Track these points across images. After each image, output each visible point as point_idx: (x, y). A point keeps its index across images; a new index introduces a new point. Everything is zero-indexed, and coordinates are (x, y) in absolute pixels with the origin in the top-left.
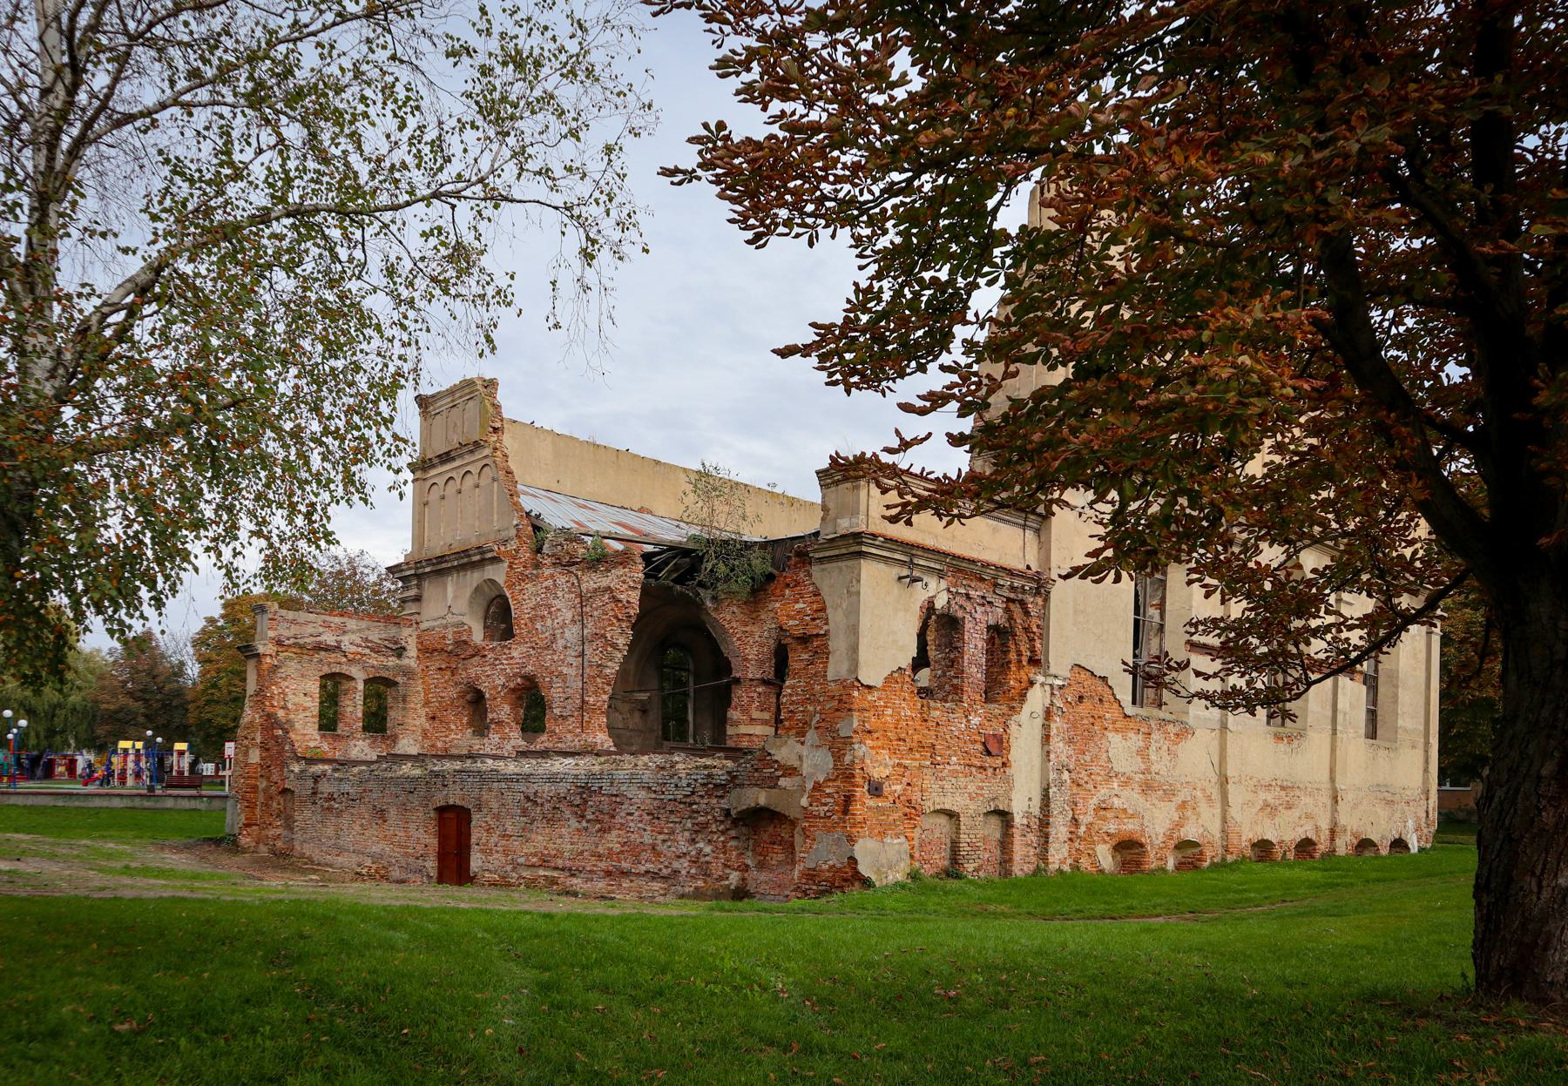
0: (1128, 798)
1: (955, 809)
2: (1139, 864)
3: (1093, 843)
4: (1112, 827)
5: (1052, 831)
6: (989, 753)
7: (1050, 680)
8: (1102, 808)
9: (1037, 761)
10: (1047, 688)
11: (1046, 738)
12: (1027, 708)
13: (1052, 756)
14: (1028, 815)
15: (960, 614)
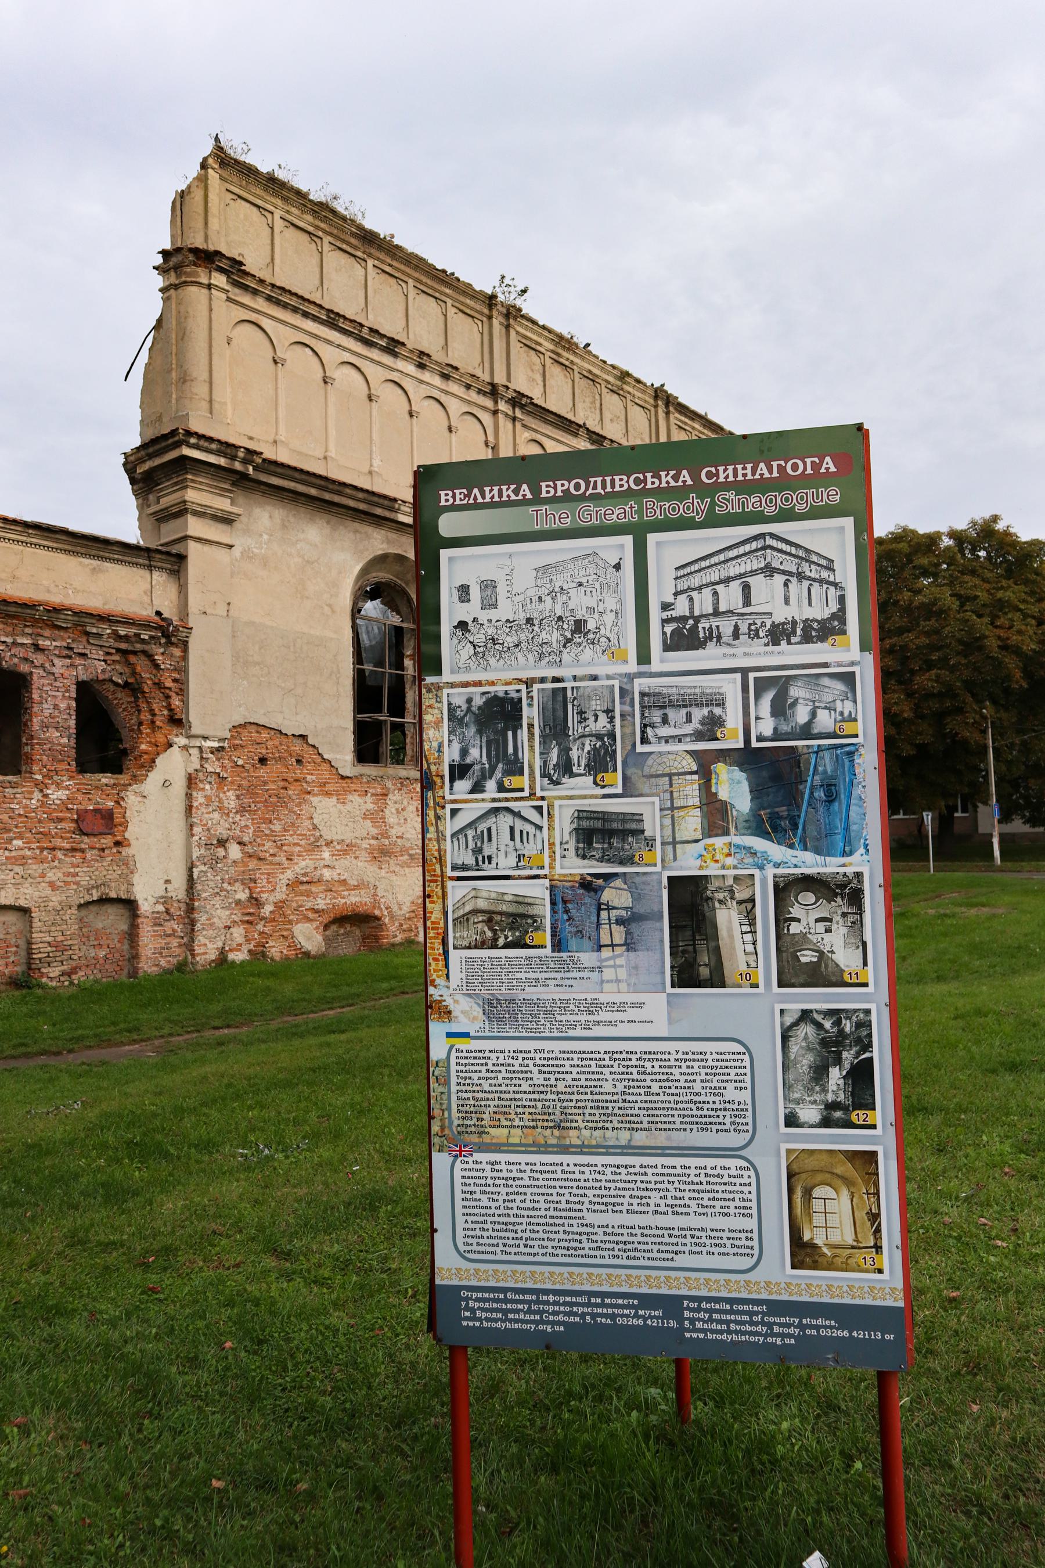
0: (357, 868)
1: (22, 903)
2: (377, 938)
3: (290, 922)
4: (321, 903)
5: (202, 918)
6: (83, 833)
7: (197, 743)
8: (301, 884)
9: (178, 836)
10: (195, 752)
11: (189, 809)
12: (154, 779)
13: (197, 830)
14: (166, 900)
15: (24, 668)
